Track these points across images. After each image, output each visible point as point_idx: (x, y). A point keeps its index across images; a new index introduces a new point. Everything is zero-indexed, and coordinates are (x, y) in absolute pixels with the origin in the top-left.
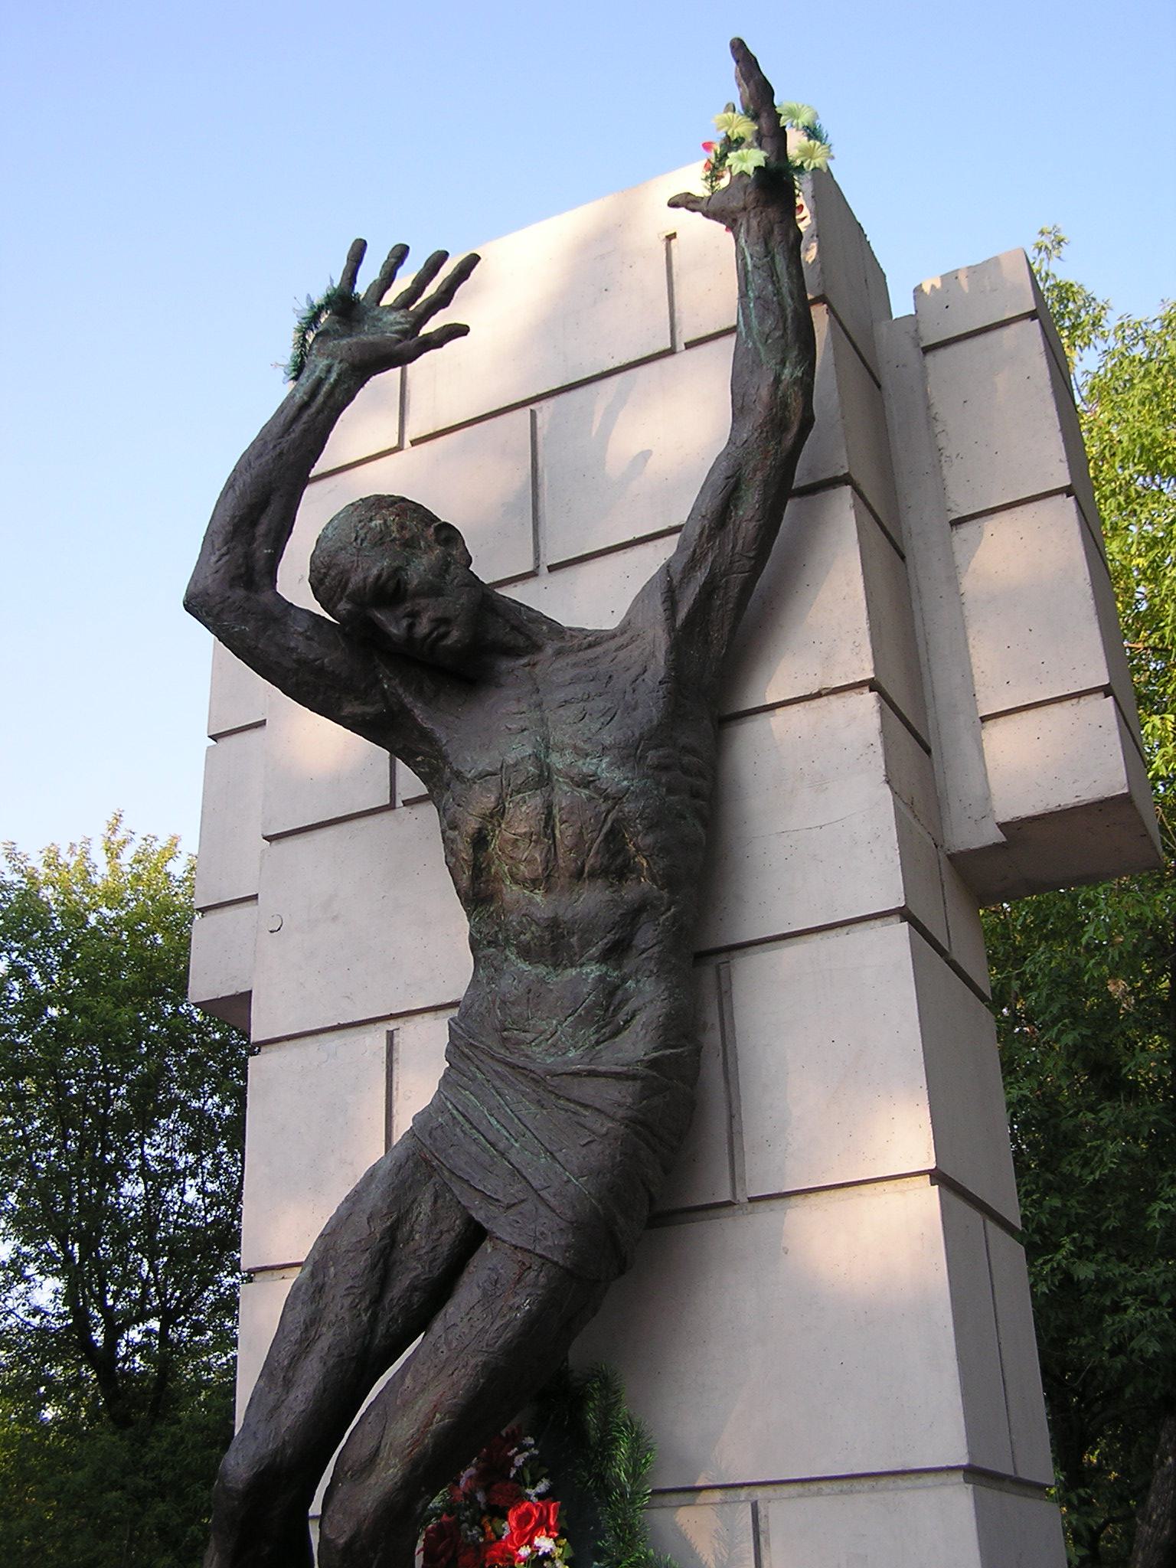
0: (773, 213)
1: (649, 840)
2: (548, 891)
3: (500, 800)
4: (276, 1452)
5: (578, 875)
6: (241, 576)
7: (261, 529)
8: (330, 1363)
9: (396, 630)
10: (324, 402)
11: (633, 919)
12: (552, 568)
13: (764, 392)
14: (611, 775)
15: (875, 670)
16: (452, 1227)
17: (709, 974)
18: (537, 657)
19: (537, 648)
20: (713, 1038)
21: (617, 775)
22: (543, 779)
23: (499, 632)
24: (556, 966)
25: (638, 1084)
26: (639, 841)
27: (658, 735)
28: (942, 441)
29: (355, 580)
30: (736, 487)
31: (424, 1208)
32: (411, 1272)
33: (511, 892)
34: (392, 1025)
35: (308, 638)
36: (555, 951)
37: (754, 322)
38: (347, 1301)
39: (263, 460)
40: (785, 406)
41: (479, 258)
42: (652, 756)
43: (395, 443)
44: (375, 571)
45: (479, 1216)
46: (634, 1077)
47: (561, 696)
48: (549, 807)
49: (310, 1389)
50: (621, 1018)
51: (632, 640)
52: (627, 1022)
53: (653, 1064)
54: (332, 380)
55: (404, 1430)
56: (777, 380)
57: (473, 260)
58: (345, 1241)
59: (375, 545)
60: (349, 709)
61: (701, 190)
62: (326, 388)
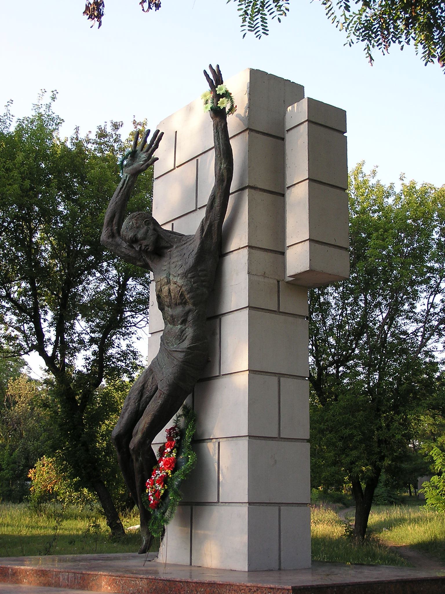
0: (218, 119)
1: (188, 296)
2: (171, 308)
3: (160, 287)
4: (119, 432)
5: (176, 304)
6: (110, 235)
7: (114, 222)
8: (129, 413)
10: (126, 186)
11: (187, 314)
12: (199, 208)
14: (180, 282)
15: (248, 243)
17: (218, 320)
18: (171, 249)
19: (172, 246)
20: (218, 336)
23: (164, 244)
24: (174, 325)
25: (185, 353)
26: (187, 296)
27: (194, 268)
30: (214, 198)
31: (151, 380)
32: (147, 394)
33: (166, 308)
35: (126, 249)
36: (173, 322)
38: (133, 401)
40: (223, 175)
41: (163, 133)
42: (189, 275)
43: (173, 168)
44: (130, 237)
46: (183, 352)
48: (169, 289)
49: (125, 419)
50: (184, 337)
51: (194, 241)
52: (185, 338)
53: (188, 348)
54: (127, 180)
55: (141, 426)
56: (220, 168)
57: (163, 134)
59: (130, 229)
62: (126, 182)
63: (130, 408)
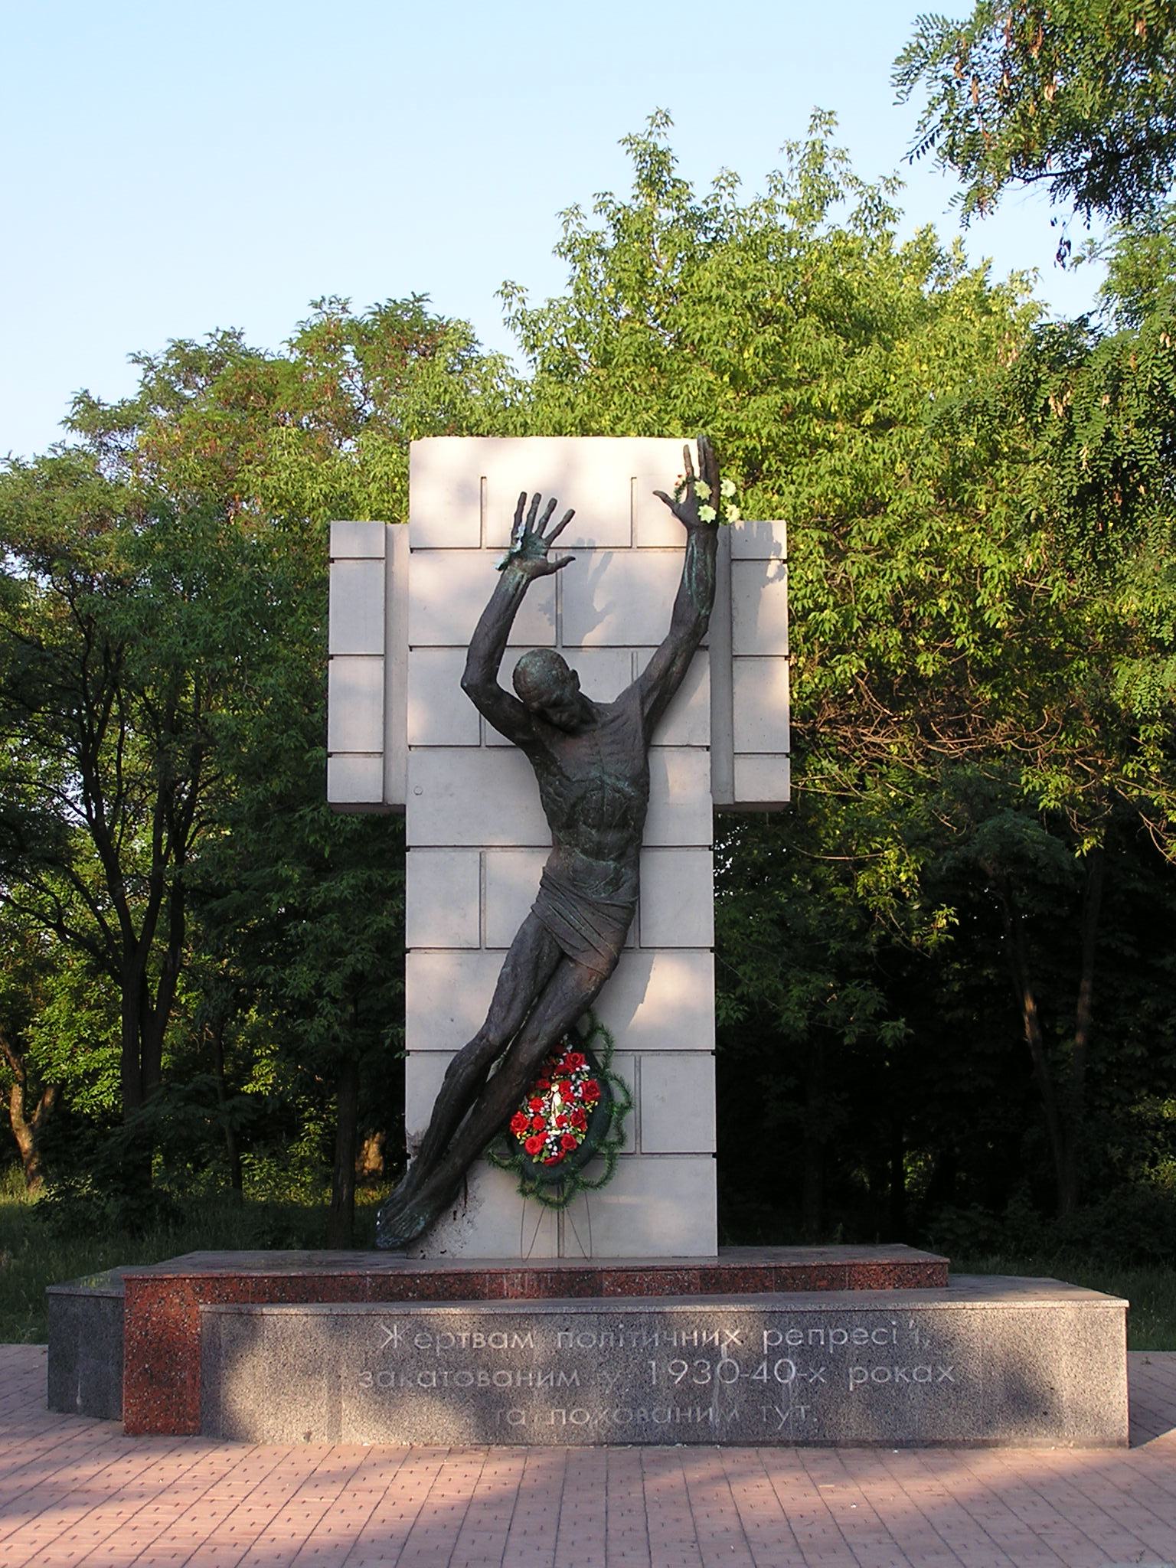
5: (610, 827)
9: (556, 718)
13: (693, 619)
16: (556, 954)
21: (630, 790)
22: (601, 788)
28: (735, 613)
29: (544, 699)
31: (546, 949)
33: (583, 828)
34: (481, 849)
37: (694, 585)
39: (501, 623)
40: (700, 626)
45: (570, 953)
47: (606, 750)
48: (603, 798)
57: (573, 513)
58: (522, 960)
60: (520, 736)
61: (672, 496)
62: (521, 587)
63: (522, 995)
